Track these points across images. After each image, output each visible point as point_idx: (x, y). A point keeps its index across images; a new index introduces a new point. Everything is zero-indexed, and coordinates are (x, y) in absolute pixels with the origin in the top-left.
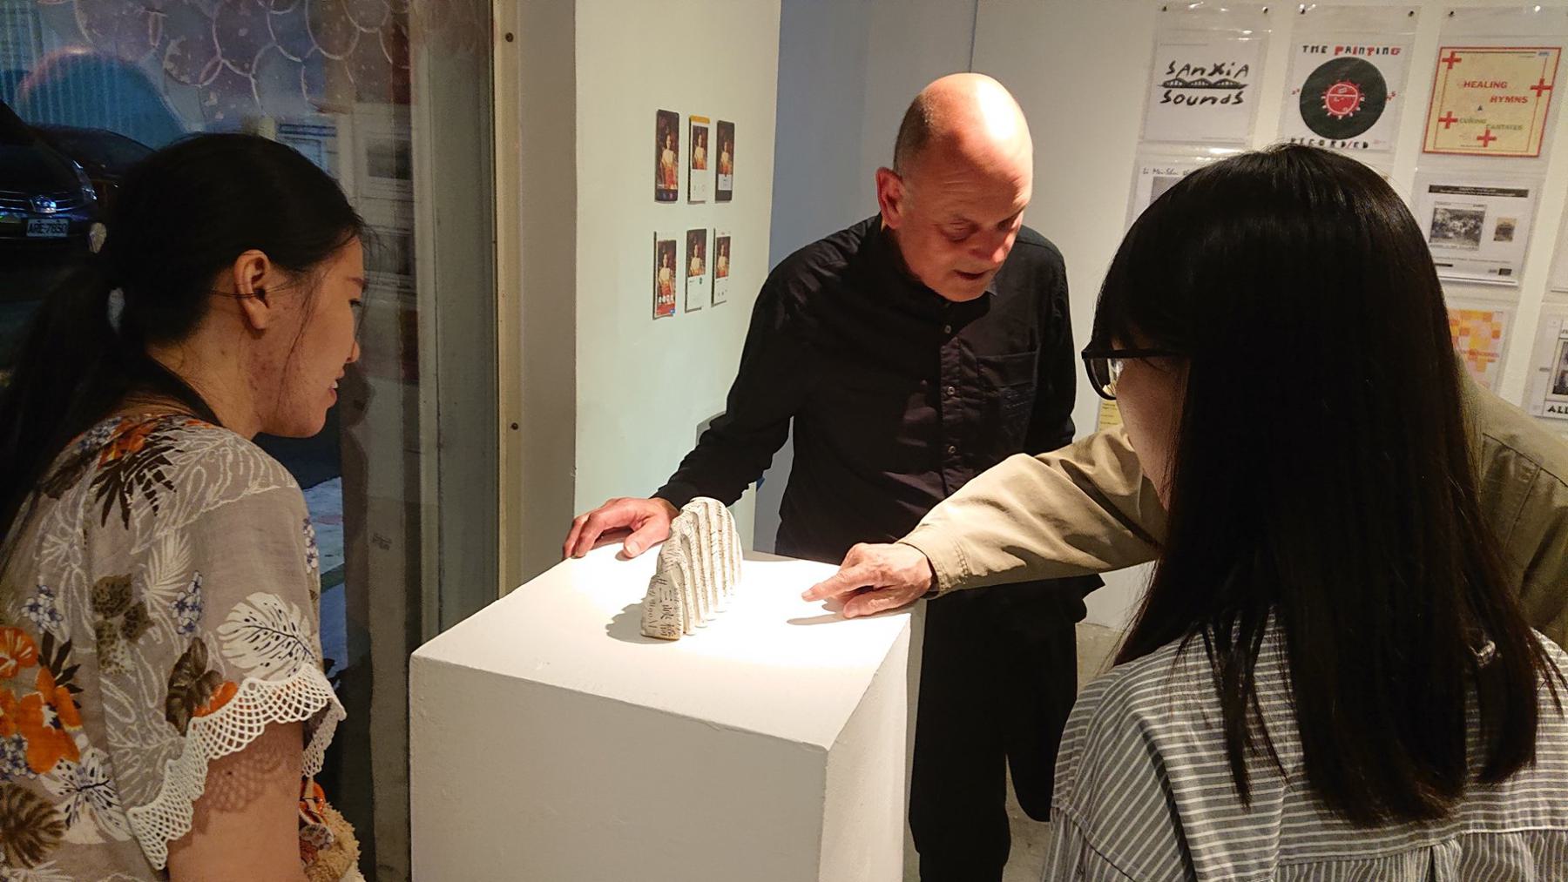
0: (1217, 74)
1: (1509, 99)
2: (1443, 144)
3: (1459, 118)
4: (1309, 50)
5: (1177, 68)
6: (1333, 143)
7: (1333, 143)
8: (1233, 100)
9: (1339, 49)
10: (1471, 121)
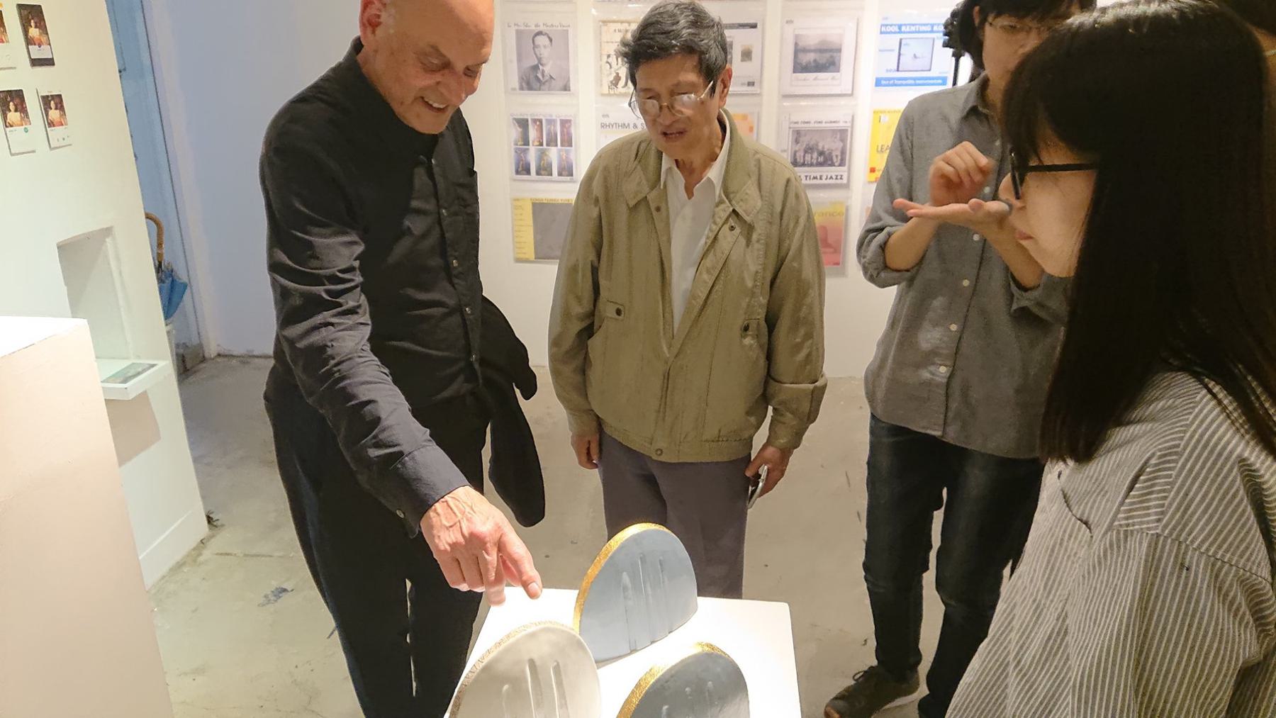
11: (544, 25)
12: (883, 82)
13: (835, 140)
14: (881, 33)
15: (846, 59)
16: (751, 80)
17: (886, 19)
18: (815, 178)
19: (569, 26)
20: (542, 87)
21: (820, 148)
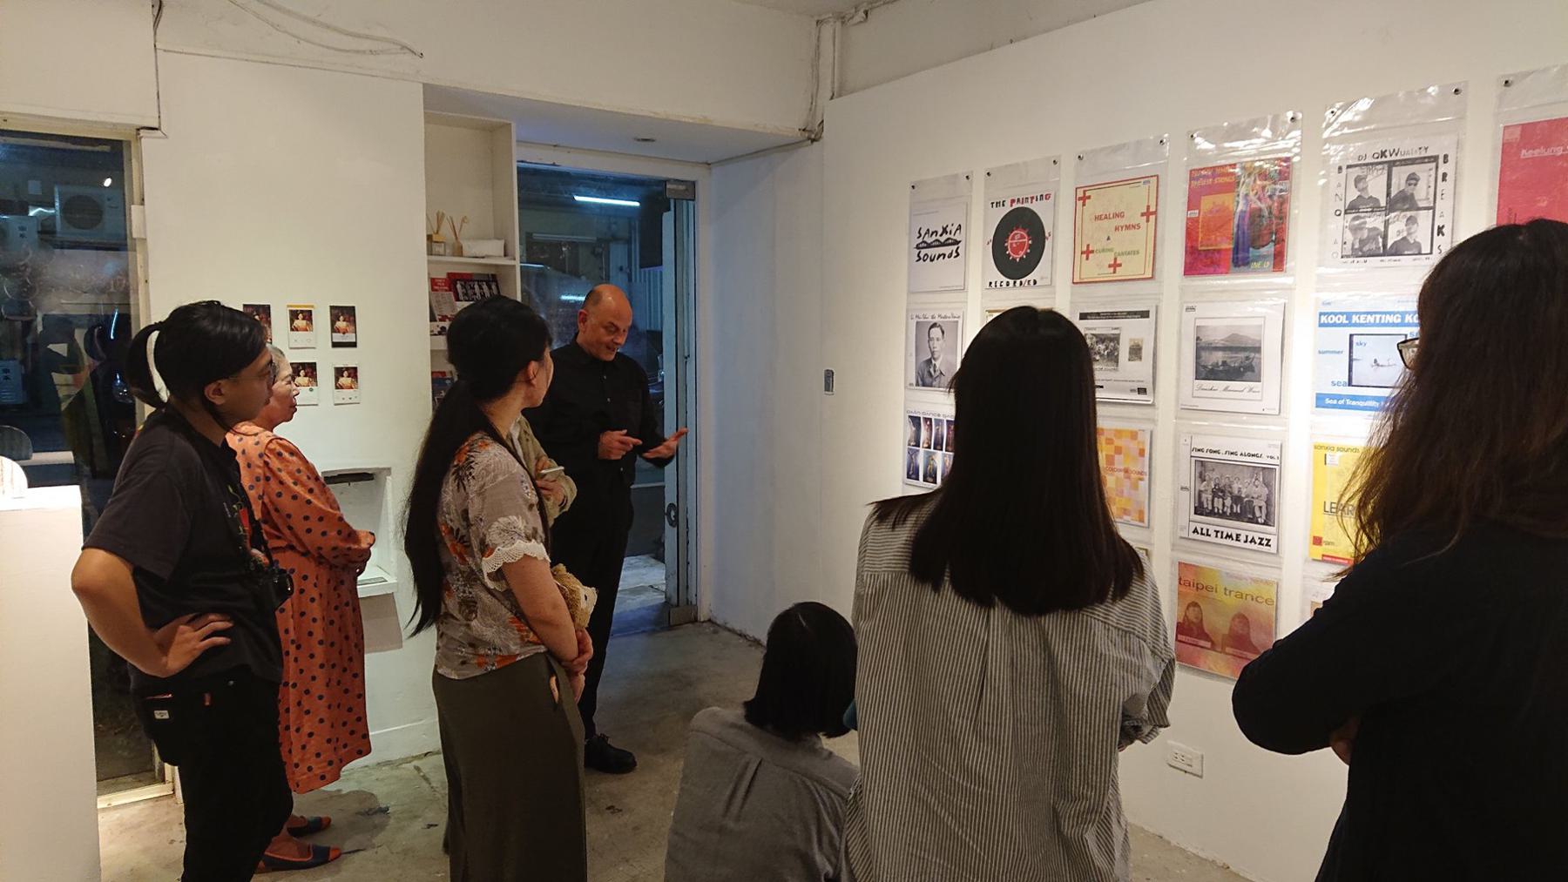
0: (944, 235)
1: (1128, 227)
2: (1086, 276)
3: (1095, 249)
4: (994, 205)
5: (923, 233)
6: (1015, 282)
7: (1015, 282)
8: (954, 254)
9: (1013, 201)
10: (1103, 250)
11: (939, 316)
12: (1328, 401)
13: (1257, 483)
14: (1321, 325)
15: (1268, 361)
16: (1142, 385)
17: (1329, 304)
18: (1230, 536)
19: (959, 317)
20: (934, 383)
21: (1236, 492)
